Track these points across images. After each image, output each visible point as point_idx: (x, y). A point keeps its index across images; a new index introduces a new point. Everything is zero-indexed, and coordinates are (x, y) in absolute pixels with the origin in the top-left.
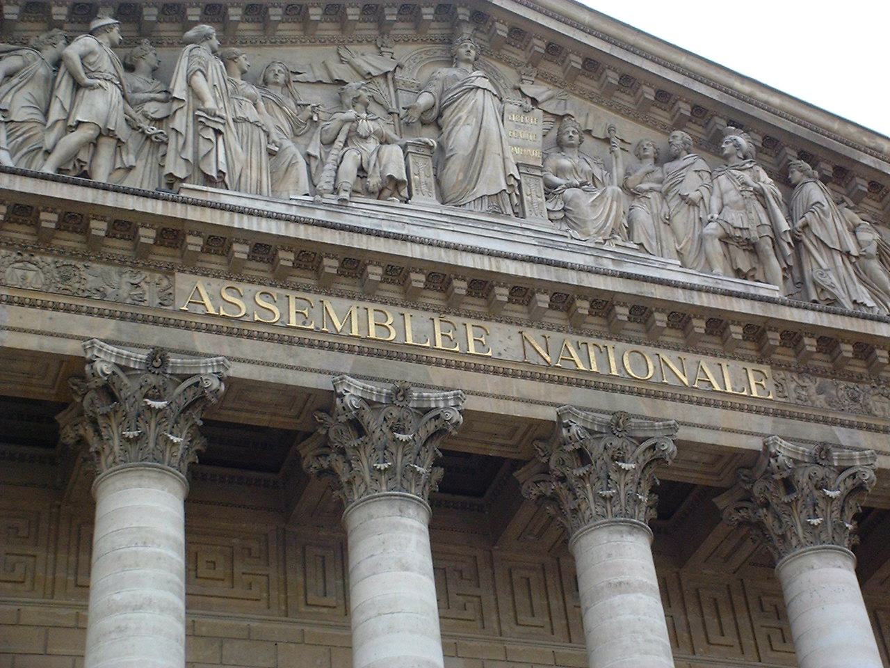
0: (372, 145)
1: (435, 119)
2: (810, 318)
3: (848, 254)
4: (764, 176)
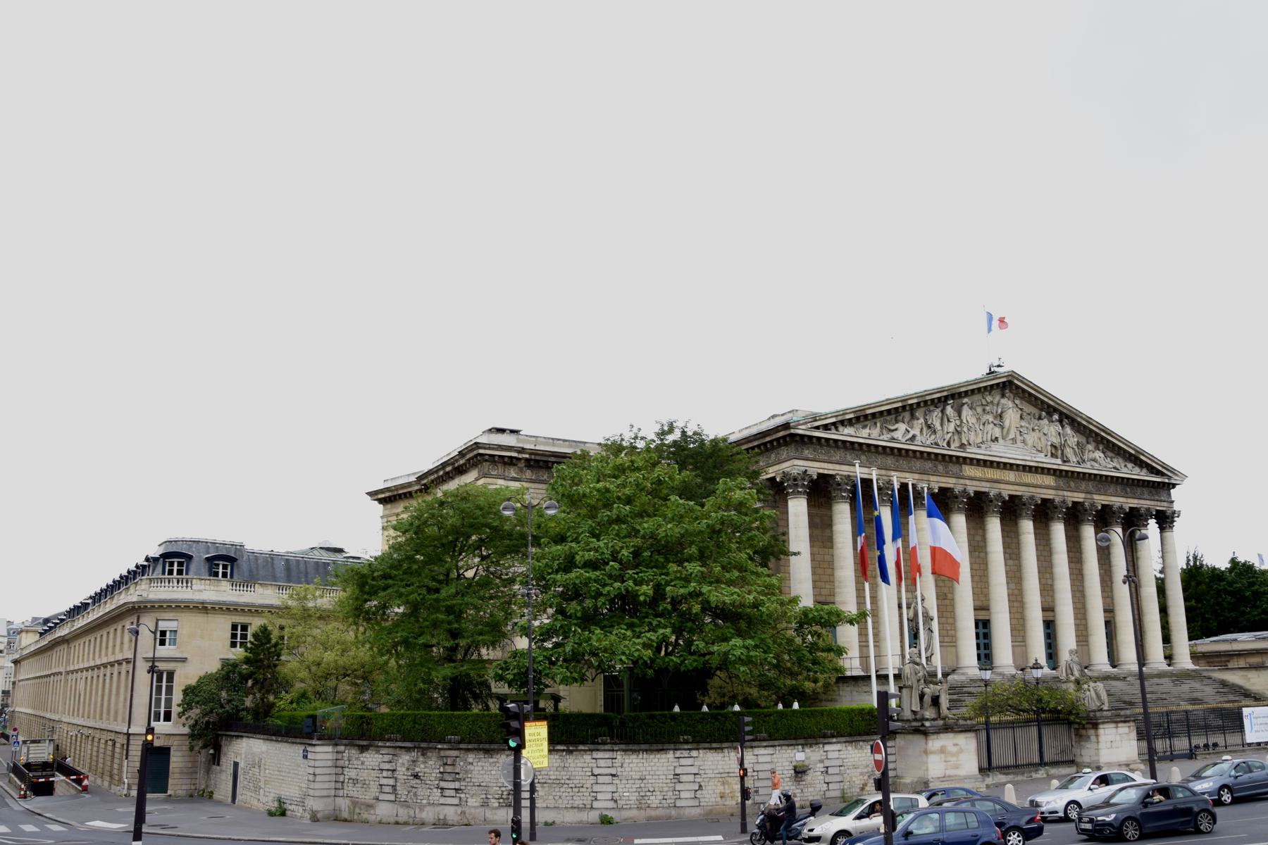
0: (991, 426)
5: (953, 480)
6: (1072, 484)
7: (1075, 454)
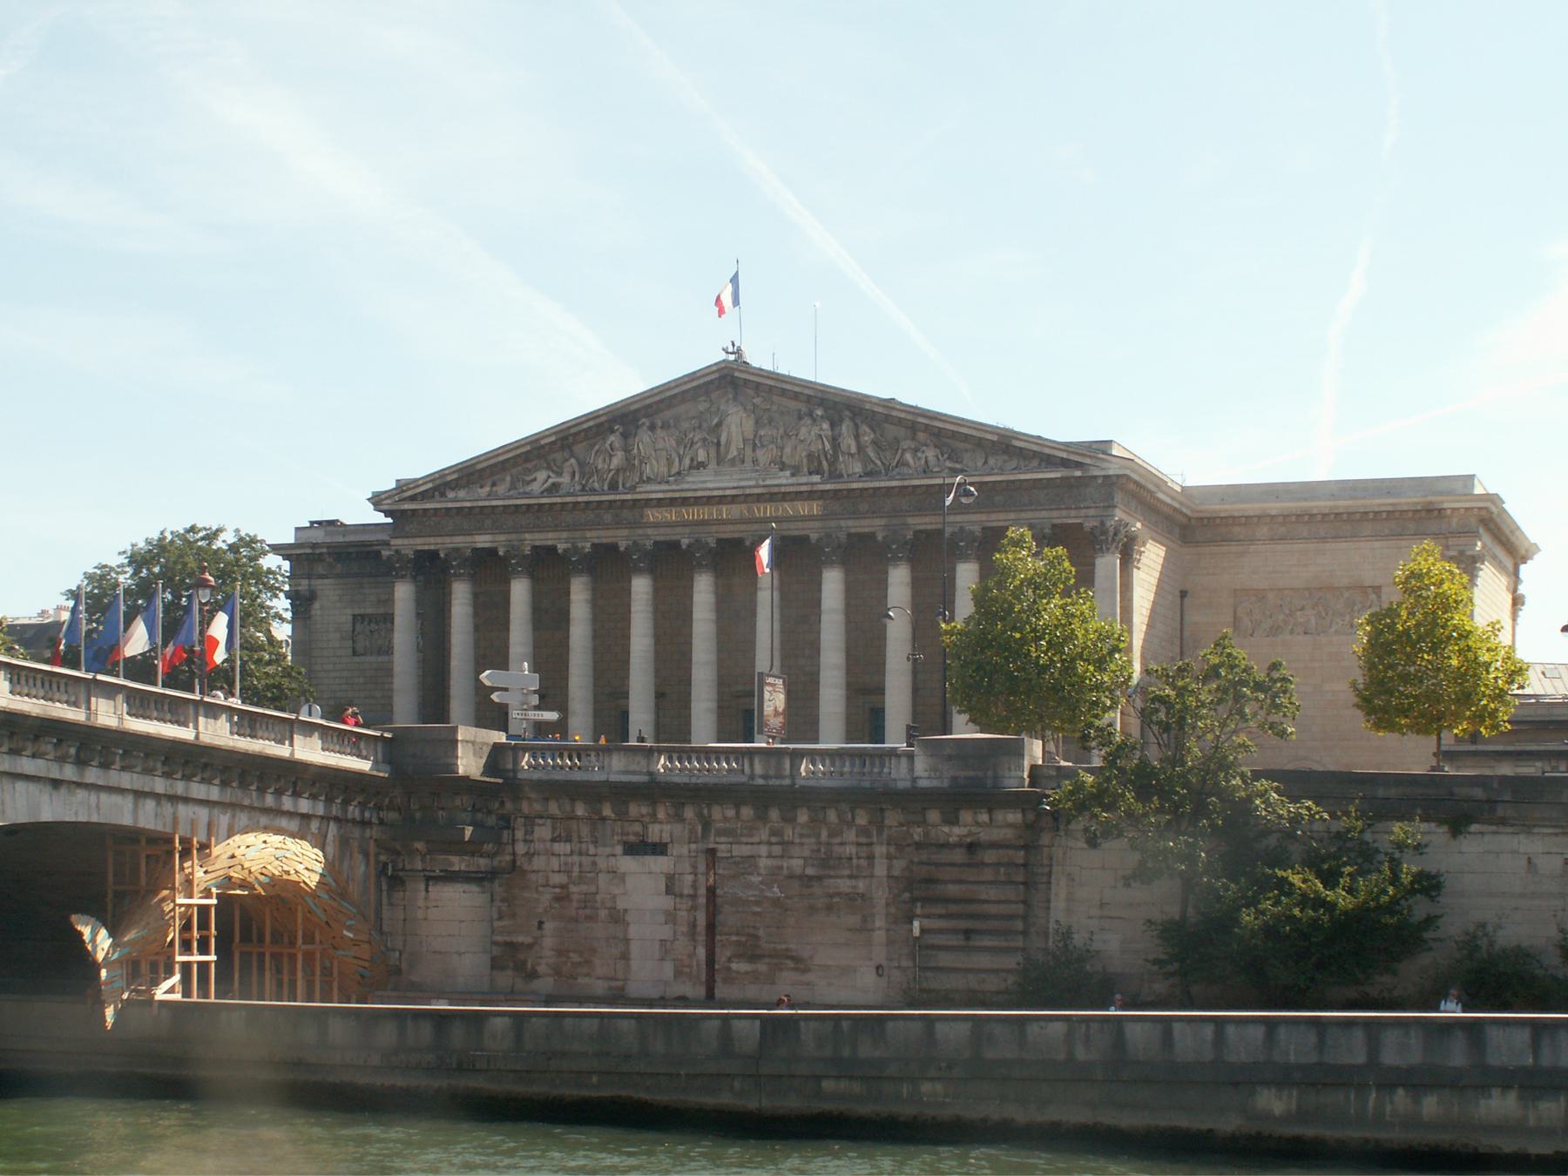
1: (719, 424)
2: (828, 487)
3: (850, 454)
4: (826, 426)
5: (625, 532)
6: (864, 507)
7: (866, 460)
